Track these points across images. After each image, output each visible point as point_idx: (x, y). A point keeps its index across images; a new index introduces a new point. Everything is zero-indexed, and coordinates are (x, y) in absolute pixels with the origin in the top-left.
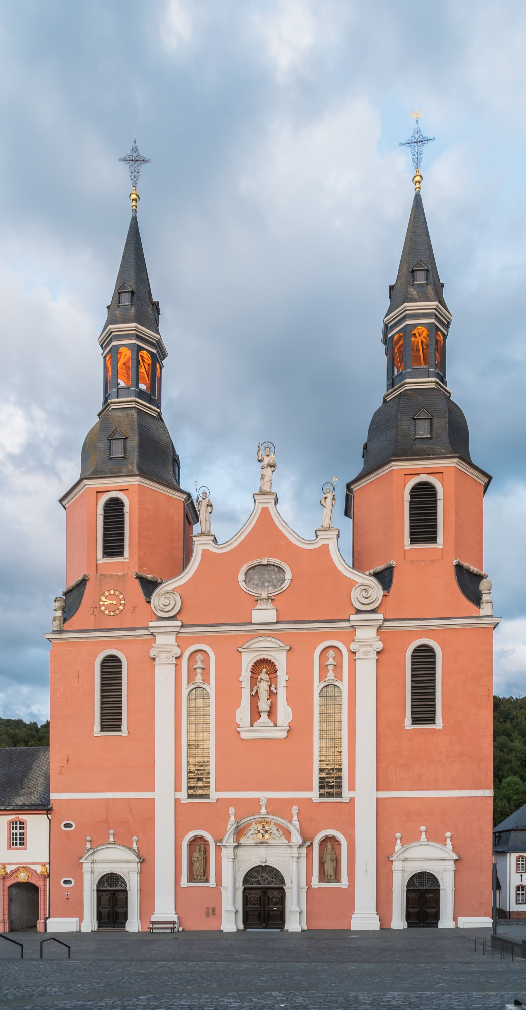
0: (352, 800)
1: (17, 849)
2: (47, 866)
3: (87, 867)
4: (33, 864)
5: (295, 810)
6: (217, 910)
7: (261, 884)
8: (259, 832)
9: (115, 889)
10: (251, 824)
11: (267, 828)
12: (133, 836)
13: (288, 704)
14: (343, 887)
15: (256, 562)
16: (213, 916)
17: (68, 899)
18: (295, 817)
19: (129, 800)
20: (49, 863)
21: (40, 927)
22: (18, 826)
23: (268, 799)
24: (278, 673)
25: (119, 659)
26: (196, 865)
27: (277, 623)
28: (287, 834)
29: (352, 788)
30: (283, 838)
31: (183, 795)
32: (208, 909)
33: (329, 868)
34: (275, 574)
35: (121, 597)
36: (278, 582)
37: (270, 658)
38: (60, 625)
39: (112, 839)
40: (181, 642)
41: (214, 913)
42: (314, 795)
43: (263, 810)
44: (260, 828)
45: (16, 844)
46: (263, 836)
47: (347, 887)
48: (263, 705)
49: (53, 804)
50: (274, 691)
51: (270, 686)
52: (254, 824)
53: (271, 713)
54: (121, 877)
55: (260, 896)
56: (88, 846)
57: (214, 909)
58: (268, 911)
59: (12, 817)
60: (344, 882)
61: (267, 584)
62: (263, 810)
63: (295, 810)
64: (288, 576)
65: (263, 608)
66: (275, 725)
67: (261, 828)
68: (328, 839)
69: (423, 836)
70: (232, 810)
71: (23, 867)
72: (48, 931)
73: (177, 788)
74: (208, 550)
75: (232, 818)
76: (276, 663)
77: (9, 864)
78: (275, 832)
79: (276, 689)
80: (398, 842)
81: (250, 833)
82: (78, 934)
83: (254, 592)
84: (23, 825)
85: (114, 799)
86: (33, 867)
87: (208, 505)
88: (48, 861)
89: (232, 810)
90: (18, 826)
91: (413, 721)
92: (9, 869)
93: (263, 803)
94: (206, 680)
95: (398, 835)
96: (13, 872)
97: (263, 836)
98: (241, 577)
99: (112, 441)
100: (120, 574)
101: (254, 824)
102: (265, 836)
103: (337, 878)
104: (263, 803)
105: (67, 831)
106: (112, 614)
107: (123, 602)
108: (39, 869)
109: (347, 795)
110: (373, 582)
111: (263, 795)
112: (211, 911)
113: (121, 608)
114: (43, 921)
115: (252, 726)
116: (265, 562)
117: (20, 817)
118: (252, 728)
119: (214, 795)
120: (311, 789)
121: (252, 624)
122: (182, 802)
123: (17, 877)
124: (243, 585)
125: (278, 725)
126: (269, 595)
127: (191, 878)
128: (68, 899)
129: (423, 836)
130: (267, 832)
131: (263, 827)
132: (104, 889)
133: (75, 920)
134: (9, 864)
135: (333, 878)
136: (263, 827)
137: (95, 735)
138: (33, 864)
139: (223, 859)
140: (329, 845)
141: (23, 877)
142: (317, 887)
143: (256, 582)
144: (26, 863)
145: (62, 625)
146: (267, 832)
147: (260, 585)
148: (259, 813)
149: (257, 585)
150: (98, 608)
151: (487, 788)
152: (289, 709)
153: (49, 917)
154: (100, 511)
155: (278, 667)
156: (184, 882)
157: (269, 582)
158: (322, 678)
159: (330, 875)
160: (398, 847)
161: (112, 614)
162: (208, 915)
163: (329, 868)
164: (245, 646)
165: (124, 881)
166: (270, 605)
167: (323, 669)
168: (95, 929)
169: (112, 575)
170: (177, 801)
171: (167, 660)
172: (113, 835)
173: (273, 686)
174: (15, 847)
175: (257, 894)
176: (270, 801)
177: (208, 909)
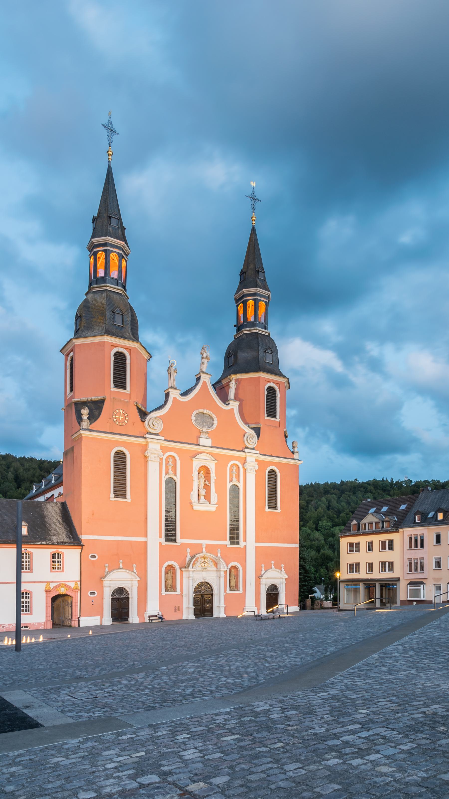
0: (245, 547)
1: (57, 572)
2: (79, 583)
3: (106, 583)
4: (69, 581)
5: (219, 551)
6: (180, 608)
7: (201, 592)
8: (203, 563)
9: (122, 597)
10: (198, 558)
11: (206, 561)
12: (133, 564)
13: (216, 492)
14: (240, 593)
15: (200, 411)
16: (179, 611)
17: (93, 604)
18: (219, 555)
19: (131, 542)
20: (80, 581)
21: (74, 623)
22: (57, 556)
23: (206, 545)
24: (211, 475)
25: (124, 454)
26: (169, 582)
27: (212, 447)
28: (216, 564)
29: (245, 540)
30: (213, 566)
31: (163, 540)
32: (175, 607)
33: (233, 582)
34: (208, 419)
35: (126, 415)
36: (210, 424)
37: (207, 466)
38: (88, 425)
39: (121, 566)
40: (164, 449)
41: (179, 610)
42: (227, 543)
43: (204, 550)
44: (203, 560)
45: (56, 569)
46: (204, 565)
47: (242, 593)
48: (203, 492)
49: (83, 543)
50: (208, 484)
51: (205, 481)
52: (200, 558)
53: (208, 497)
54: (125, 589)
55: (200, 600)
56: (107, 570)
57: (179, 607)
58: (204, 607)
59: (53, 550)
60: (241, 591)
61: (204, 424)
62: (204, 550)
63: (219, 551)
64: (216, 422)
65: (205, 437)
66: (210, 504)
67: (203, 560)
68: (235, 567)
69: (273, 566)
70: (188, 550)
71: (63, 584)
72: (81, 626)
73: (160, 537)
74: (176, 398)
75: (188, 555)
76: (210, 469)
77: (52, 582)
78: (211, 563)
79: (210, 483)
80: (263, 569)
81: (199, 563)
82: (101, 627)
83: (199, 428)
84: (60, 555)
85: (122, 541)
86: (69, 584)
87: (174, 371)
88: (79, 580)
89: (188, 550)
90: (57, 556)
91: (269, 507)
92: (52, 585)
93: (204, 546)
94: (176, 474)
95: (263, 565)
96: (55, 587)
97: (204, 565)
98: (193, 418)
99: (115, 314)
100: (125, 400)
101: (200, 558)
102: (205, 565)
103: (237, 588)
104: (204, 546)
105: (93, 560)
106: (120, 424)
107: (127, 418)
108: (72, 585)
109: (242, 543)
110: (253, 432)
111: (205, 542)
112: (177, 608)
113: (126, 422)
114: (77, 620)
115: (198, 503)
116: (205, 411)
117: (60, 550)
118: (198, 504)
119: (179, 541)
120: (227, 540)
121: (199, 445)
122: (162, 544)
123: (59, 590)
124: (194, 422)
125: (211, 503)
126: (207, 431)
127: (167, 590)
128: (93, 604)
129: (273, 566)
130: (206, 563)
131: (205, 560)
132: (115, 597)
133: (98, 618)
134: (52, 582)
135: (235, 588)
136: (205, 560)
137: (111, 500)
138: (69, 581)
139: (184, 578)
140: (233, 570)
141: (62, 591)
142: (229, 593)
143: (199, 422)
144: (64, 582)
145: (89, 426)
146: (206, 563)
147: (201, 423)
148: (202, 552)
149: (200, 423)
150: (112, 419)
151: (296, 543)
152: (216, 495)
153: (80, 617)
154: (112, 358)
155: (211, 471)
156: (163, 592)
157: (205, 423)
158: (231, 480)
159: (234, 587)
160: (263, 572)
161: (120, 424)
162: (175, 611)
163: (233, 582)
164: (196, 457)
165: (127, 592)
166: (207, 436)
167: (231, 475)
168: (112, 623)
169: (120, 400)
170: (160, 543)
171: (155, 459)
172: (122, 563)
173: (207, 481)
174: (54, 570)
175: (199, 598)
176: (207, 545)
177: (175, 607)
